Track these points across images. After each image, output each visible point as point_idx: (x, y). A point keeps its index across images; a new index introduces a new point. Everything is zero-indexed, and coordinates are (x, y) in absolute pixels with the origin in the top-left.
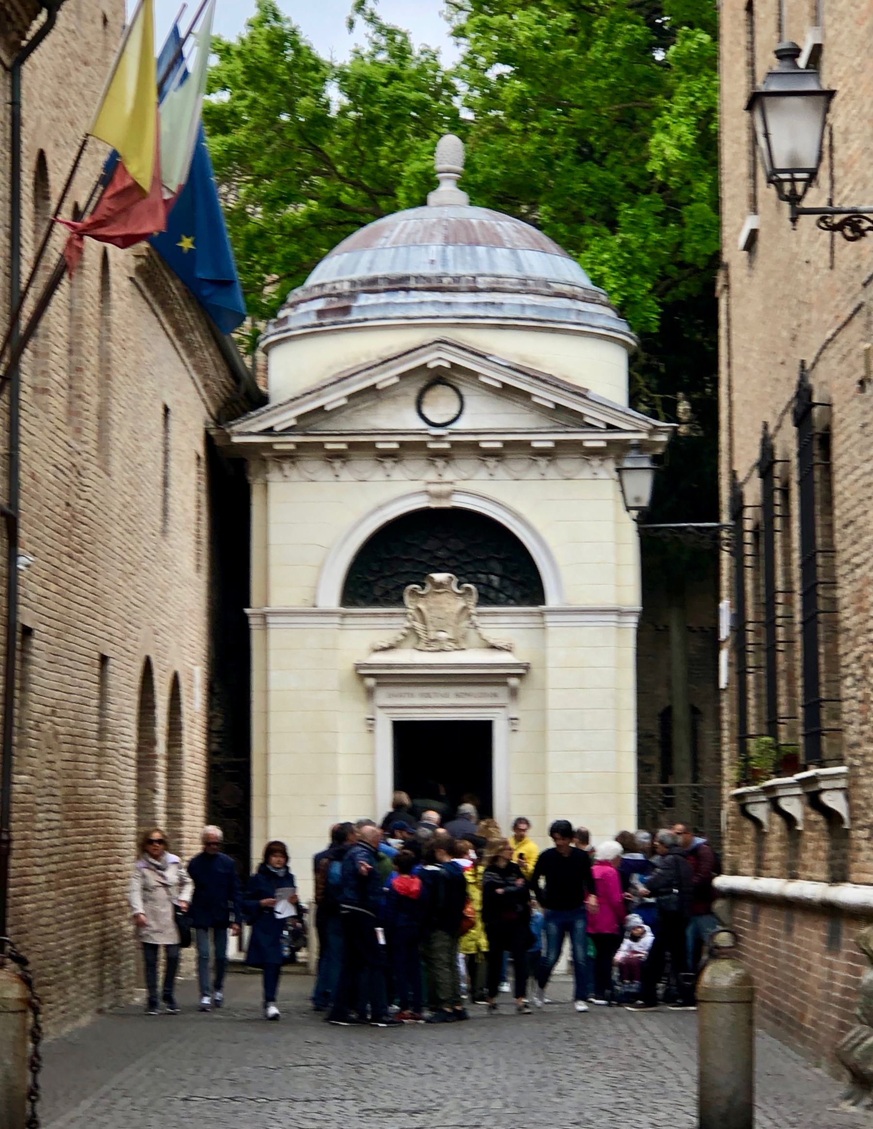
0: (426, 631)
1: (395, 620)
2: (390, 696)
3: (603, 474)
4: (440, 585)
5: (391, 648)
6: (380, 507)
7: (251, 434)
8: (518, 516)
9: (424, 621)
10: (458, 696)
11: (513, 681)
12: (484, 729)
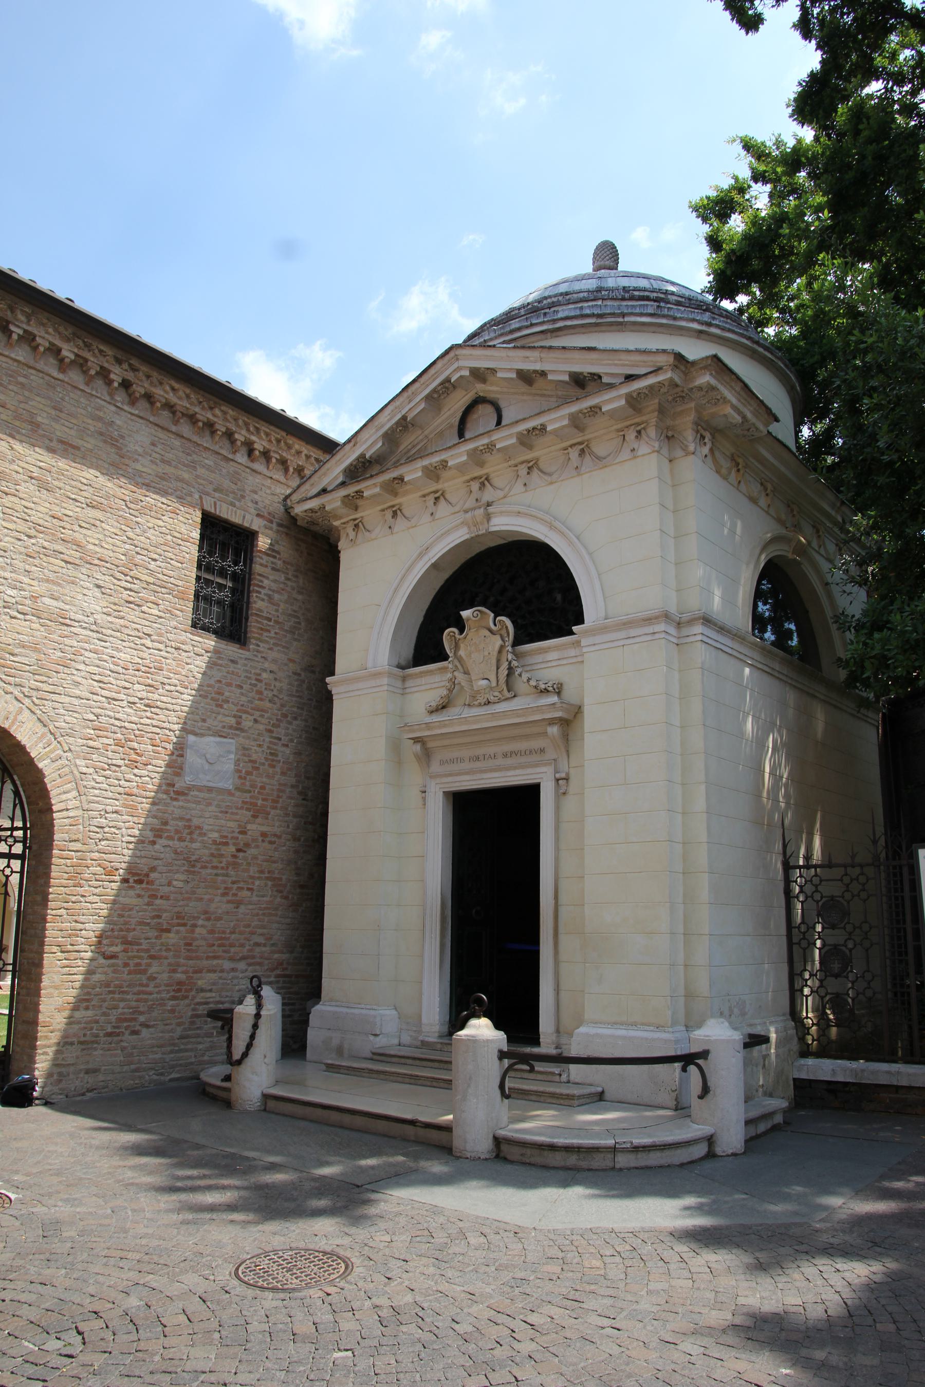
2: (442, 763)
3: (643, 448)
5: (443, 707)
7: (307, 499)
9: (466, 673)
10: (505, 755)
11: (554, 730)
12: (529, 795)
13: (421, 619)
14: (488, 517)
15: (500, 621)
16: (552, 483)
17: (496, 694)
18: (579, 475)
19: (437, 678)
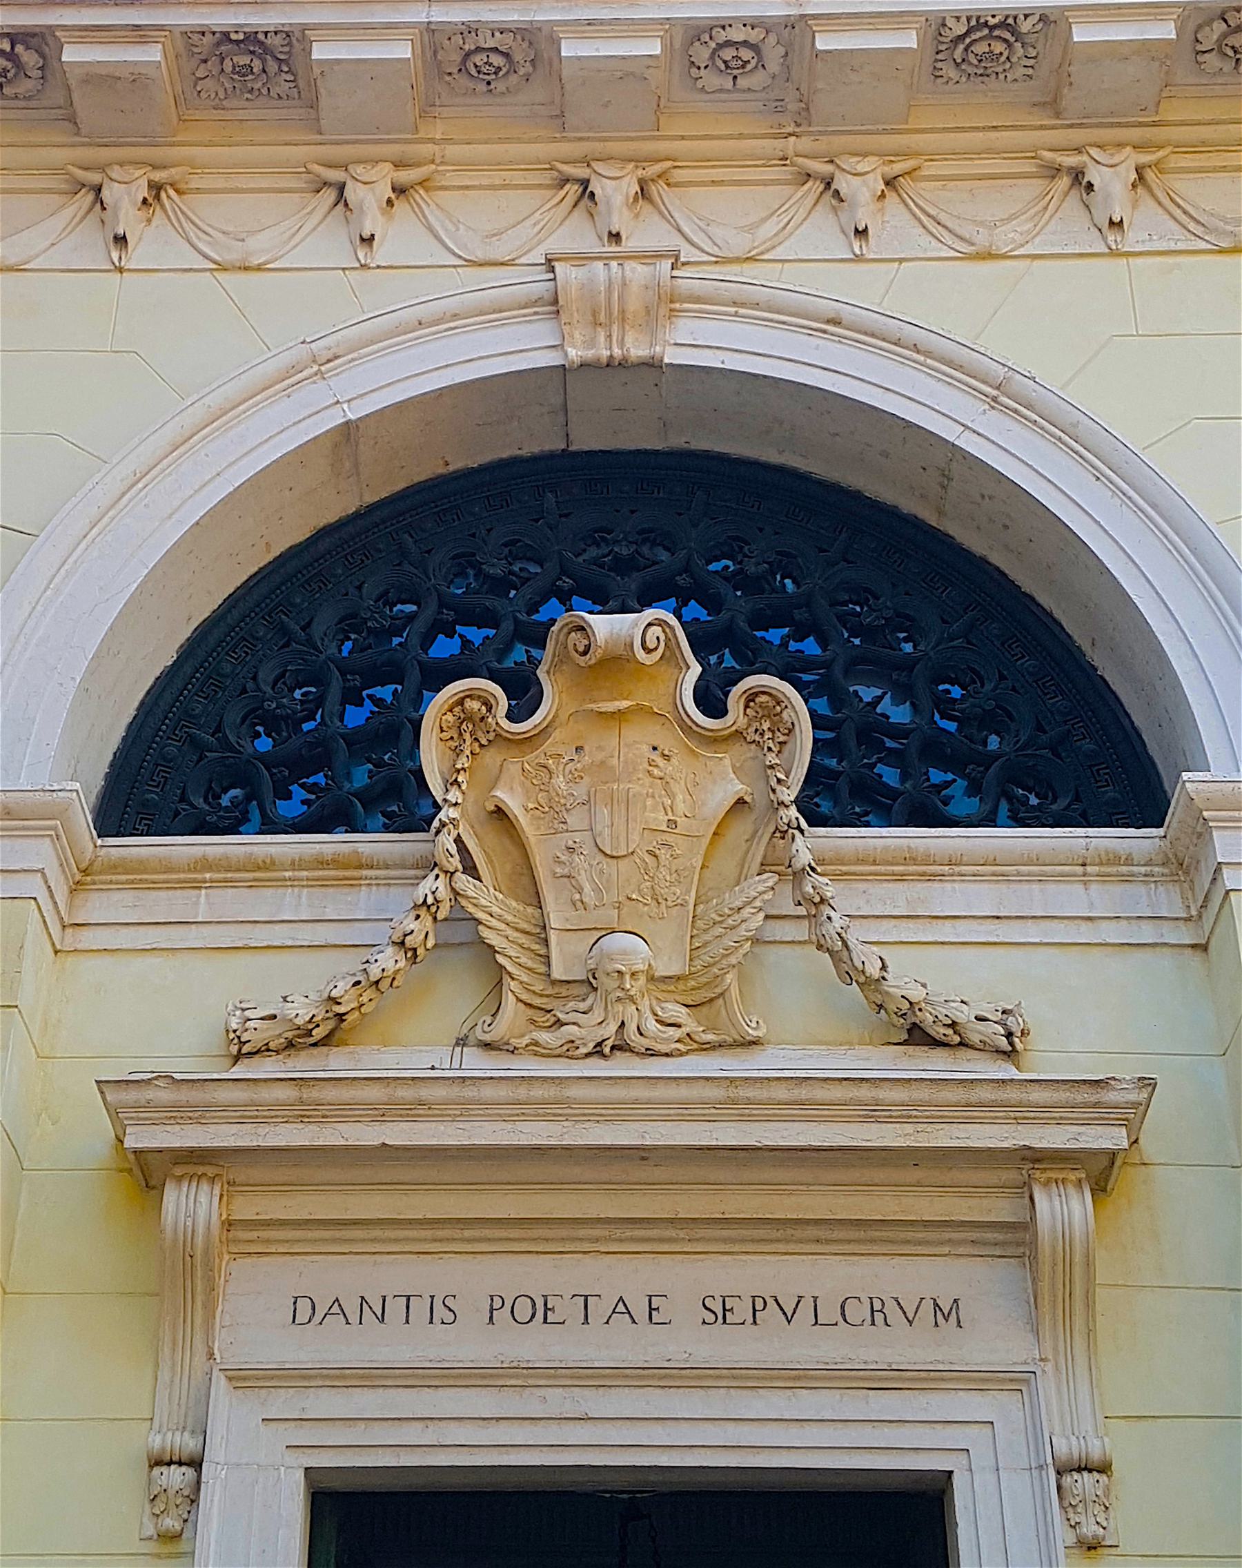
0: (542, 934)
1: (362, 901)
2: (305, 1312)
4: (616, 665)
6: (322, 364)
8: (1001, 393)
13: (168, 657)
14: (667, 304)
15: (751, 697)
16: (988, 256)
17: (675, 1011)
18: (1113, 253)
19: (293, 902)
